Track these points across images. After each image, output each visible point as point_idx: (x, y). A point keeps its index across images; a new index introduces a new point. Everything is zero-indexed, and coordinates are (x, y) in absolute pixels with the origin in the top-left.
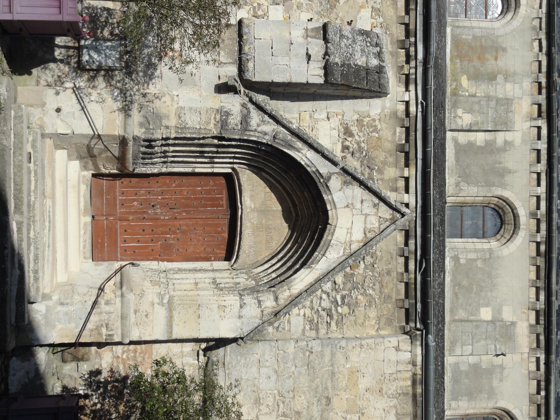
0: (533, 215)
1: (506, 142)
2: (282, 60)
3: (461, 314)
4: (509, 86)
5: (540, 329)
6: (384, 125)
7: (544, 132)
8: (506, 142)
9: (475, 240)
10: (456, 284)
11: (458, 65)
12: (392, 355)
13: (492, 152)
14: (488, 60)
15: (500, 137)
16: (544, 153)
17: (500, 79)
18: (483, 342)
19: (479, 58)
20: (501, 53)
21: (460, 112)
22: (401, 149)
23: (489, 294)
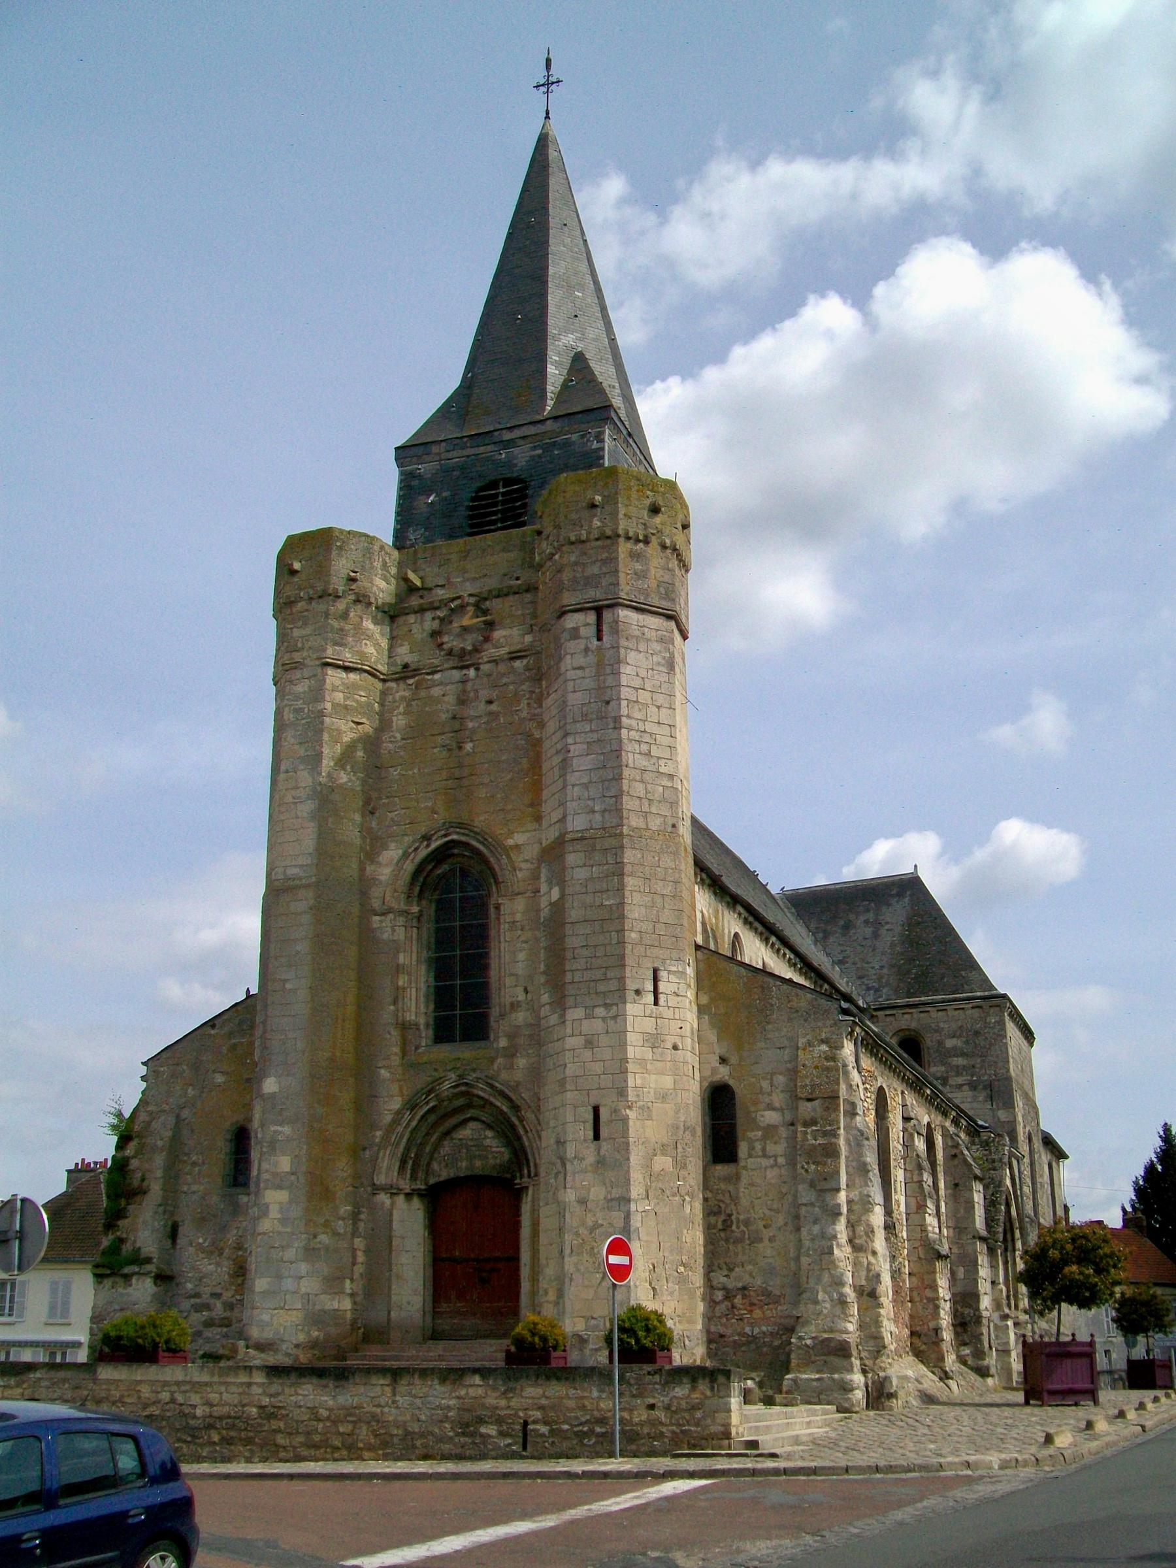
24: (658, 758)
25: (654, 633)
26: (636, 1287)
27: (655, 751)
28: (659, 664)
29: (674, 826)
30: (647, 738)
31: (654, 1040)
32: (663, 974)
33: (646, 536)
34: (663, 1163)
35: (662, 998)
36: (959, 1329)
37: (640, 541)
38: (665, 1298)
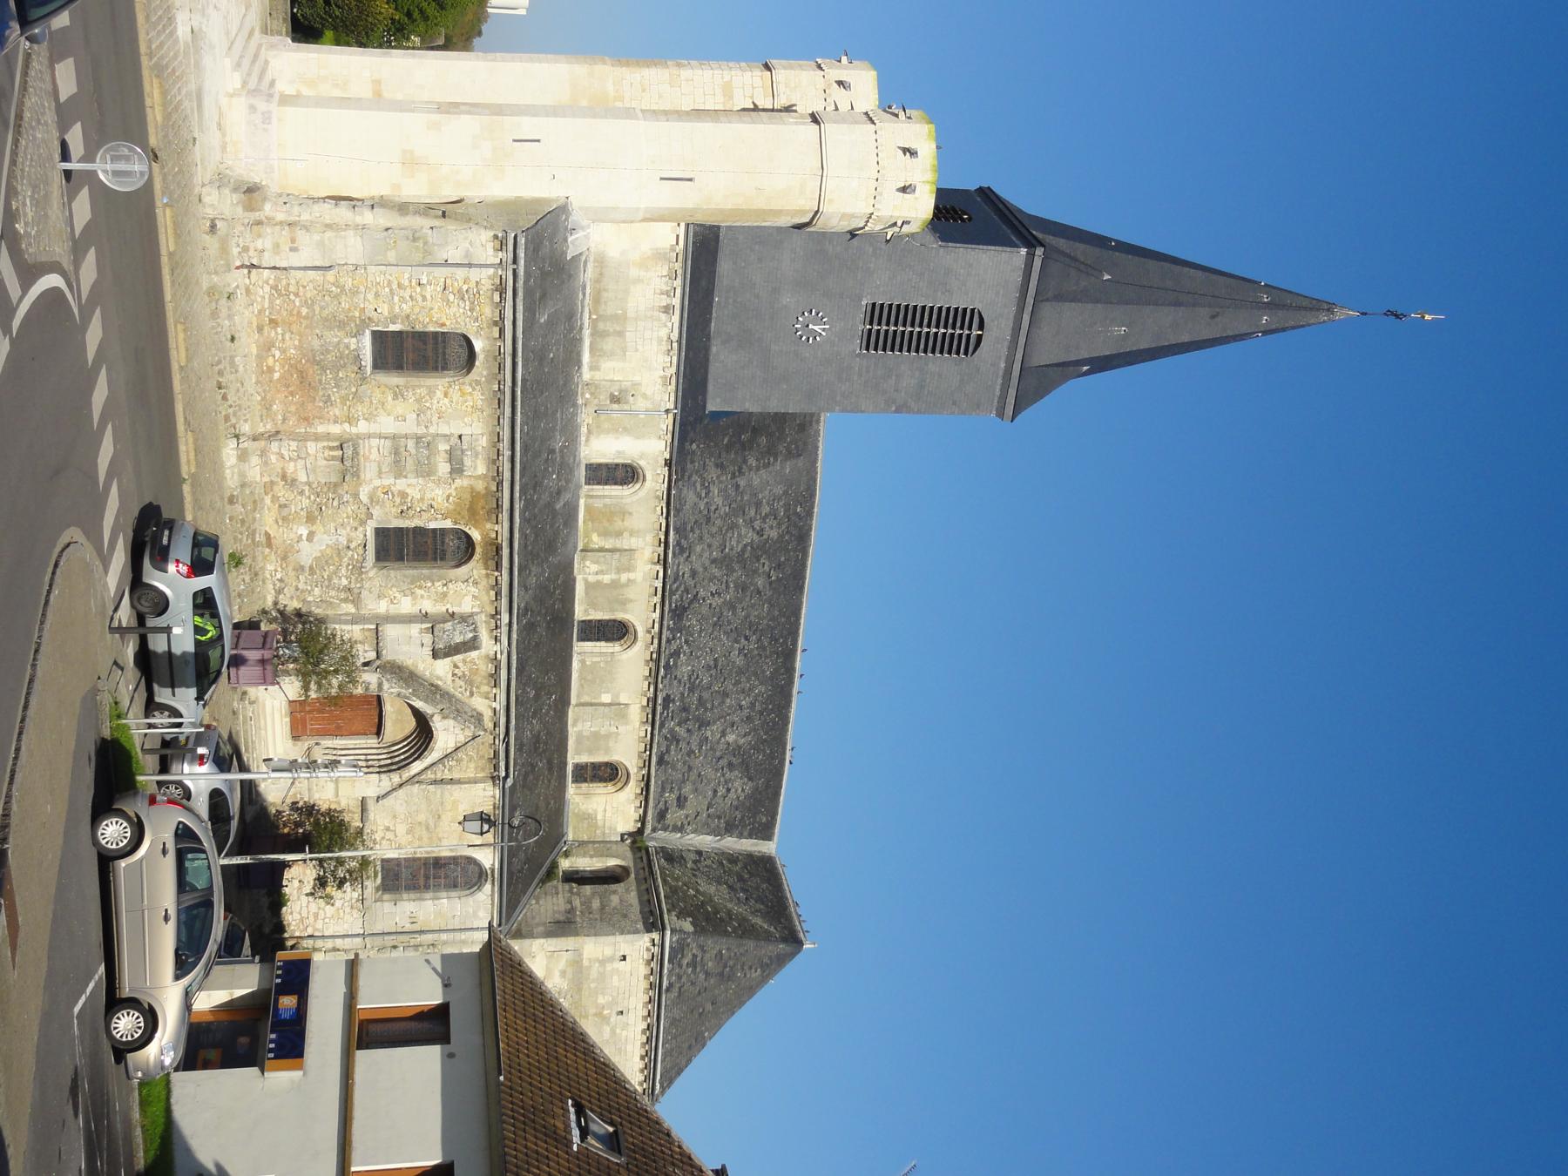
2: (405, 648)
3: (586, 699)
4: (633, 540)
5: (649, 710)
7: (661, 574)
10: (581, 678)
12: (481, 793)
15: (624, 577)
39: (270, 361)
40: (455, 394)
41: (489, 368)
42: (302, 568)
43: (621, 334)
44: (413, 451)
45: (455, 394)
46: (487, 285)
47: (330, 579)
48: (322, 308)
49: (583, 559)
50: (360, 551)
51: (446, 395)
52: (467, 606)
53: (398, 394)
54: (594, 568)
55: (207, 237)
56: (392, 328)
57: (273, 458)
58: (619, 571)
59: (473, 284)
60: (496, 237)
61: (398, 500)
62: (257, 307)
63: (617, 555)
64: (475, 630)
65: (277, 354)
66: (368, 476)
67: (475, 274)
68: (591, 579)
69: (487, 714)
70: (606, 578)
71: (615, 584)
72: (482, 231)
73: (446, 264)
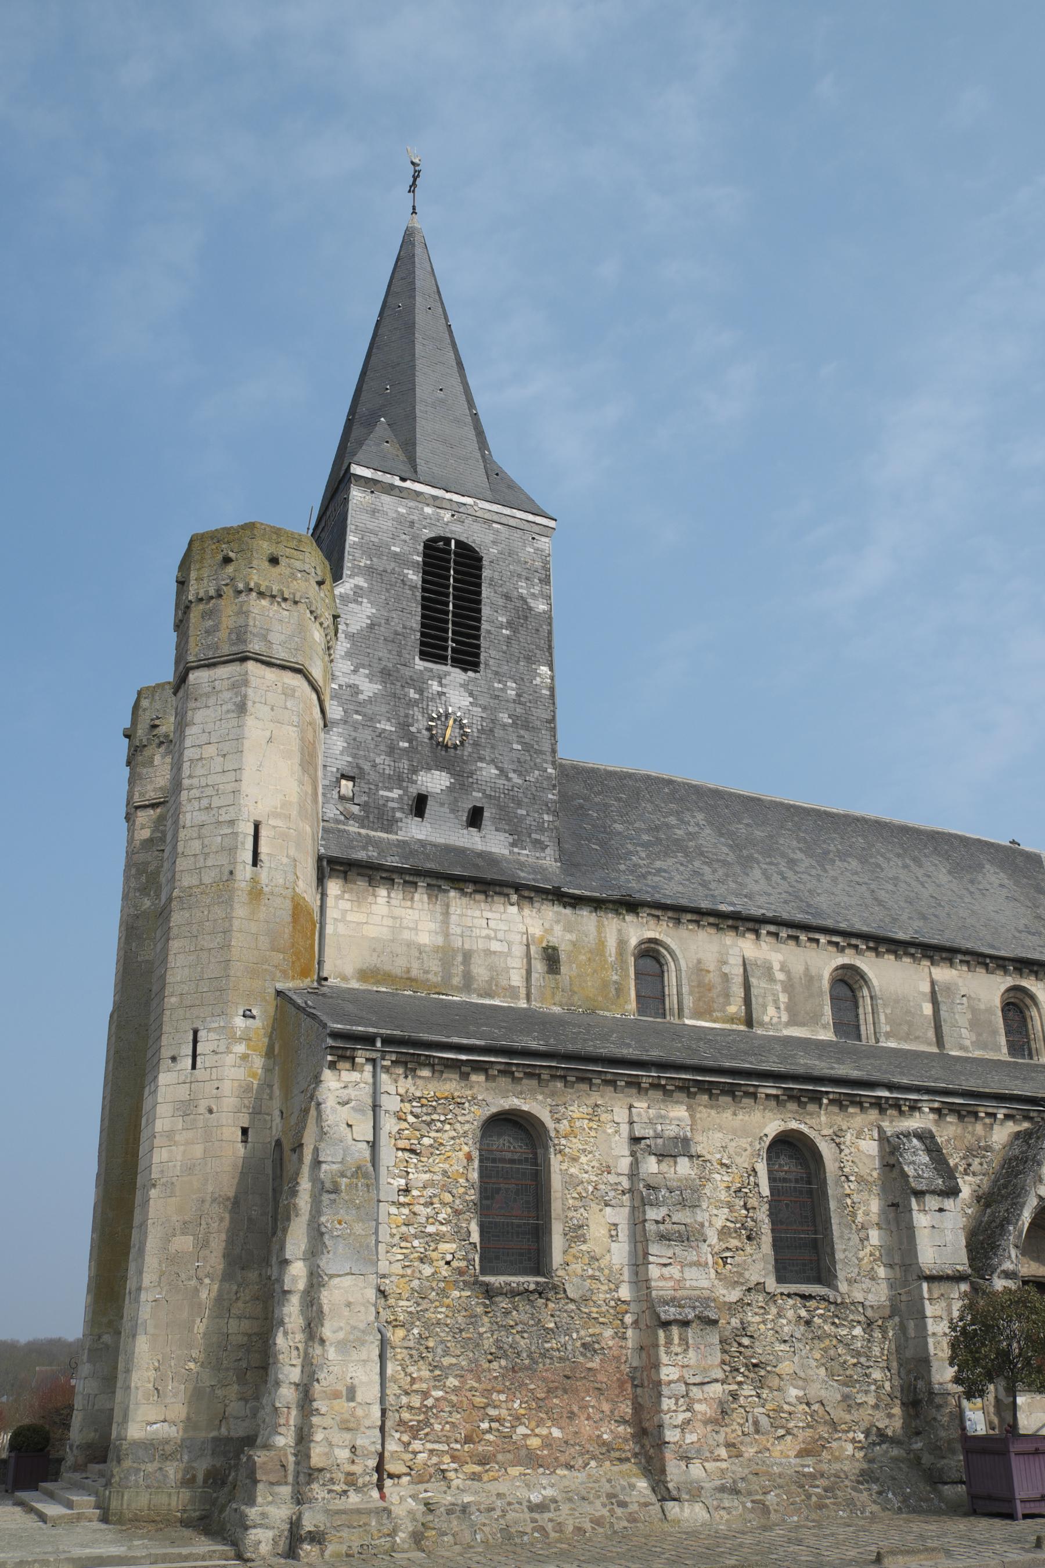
0: (841, 950)
1: (781, 970)
3: (931, 1034)
4: (732, 960)
6: (945, 1133)
7: (772, 928)
8: (781, 970)
9: (861, 1011)
10: (906, 1038)
11: (719, 1015)
13: (792, 986)
14: (710, 981)
15: (780, 976)
16: (791, 932)
17: (726, 969)
18: (957, 1017)
19: (710, 990)
20: (702, 966)
21: (766, 1019)
22: (961, 1117)
23: (912, 1004)
24: (219, 808)
25: (226, 682)
26: (137, 1388)
27: (216, 802)
28: (228, 711)
29: (231, 873)
30: (209, 791)
31: (186, 1108)
32: (202, 1034)
33: (218, 590)
34: (184, 1243)
35: (199, 1059)
36: (912, 1411)
37: (212, 598)
38: (167, 1401)
39: (534, 1442)
40: (574, 1145)
41: (533, 1092)
42: (846, 1397)
43: (467, 956)
44: (663, 1211)
45: (574, 1145)
46: (406, 1085)
47: (857, 1354)
48: (446, 1353)
49: (762, 1024)
50: (812, 1304)
51: (575, 1159)
52: (870, 1147)
53: (576, 1233)
54: (771, 1011)
55: (330, 1549)
56: (475, 1237)
57: (691, 1438)
58: (772, 979)
59: (407, 1107)
60: (332, 1066)
61: (734, 1243)
62: (447, 1463)
63: (753, 981)
64: (907, 1135)
65: (521, 1430)
66: (705, 1284)
67: (390, 1103)
68: (785, 1018)
69: (1011, 1127)
70: (783, 998)
71: (789, 987)
72: (323, 1086)
73: (374, 1145)
